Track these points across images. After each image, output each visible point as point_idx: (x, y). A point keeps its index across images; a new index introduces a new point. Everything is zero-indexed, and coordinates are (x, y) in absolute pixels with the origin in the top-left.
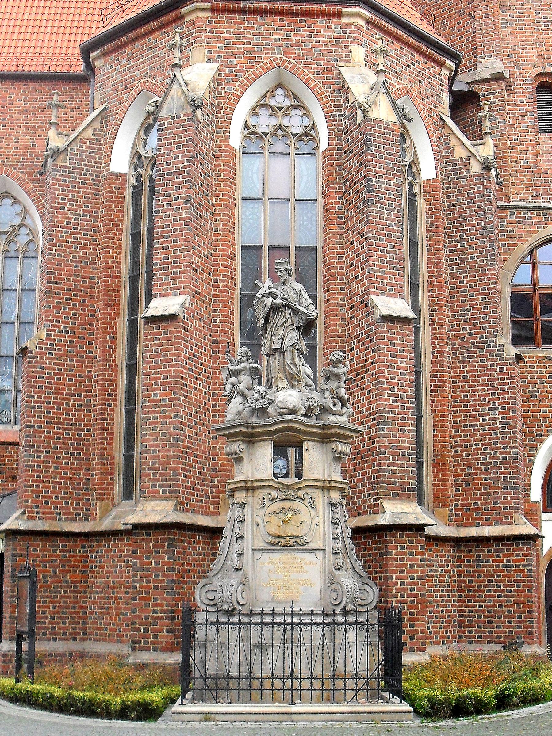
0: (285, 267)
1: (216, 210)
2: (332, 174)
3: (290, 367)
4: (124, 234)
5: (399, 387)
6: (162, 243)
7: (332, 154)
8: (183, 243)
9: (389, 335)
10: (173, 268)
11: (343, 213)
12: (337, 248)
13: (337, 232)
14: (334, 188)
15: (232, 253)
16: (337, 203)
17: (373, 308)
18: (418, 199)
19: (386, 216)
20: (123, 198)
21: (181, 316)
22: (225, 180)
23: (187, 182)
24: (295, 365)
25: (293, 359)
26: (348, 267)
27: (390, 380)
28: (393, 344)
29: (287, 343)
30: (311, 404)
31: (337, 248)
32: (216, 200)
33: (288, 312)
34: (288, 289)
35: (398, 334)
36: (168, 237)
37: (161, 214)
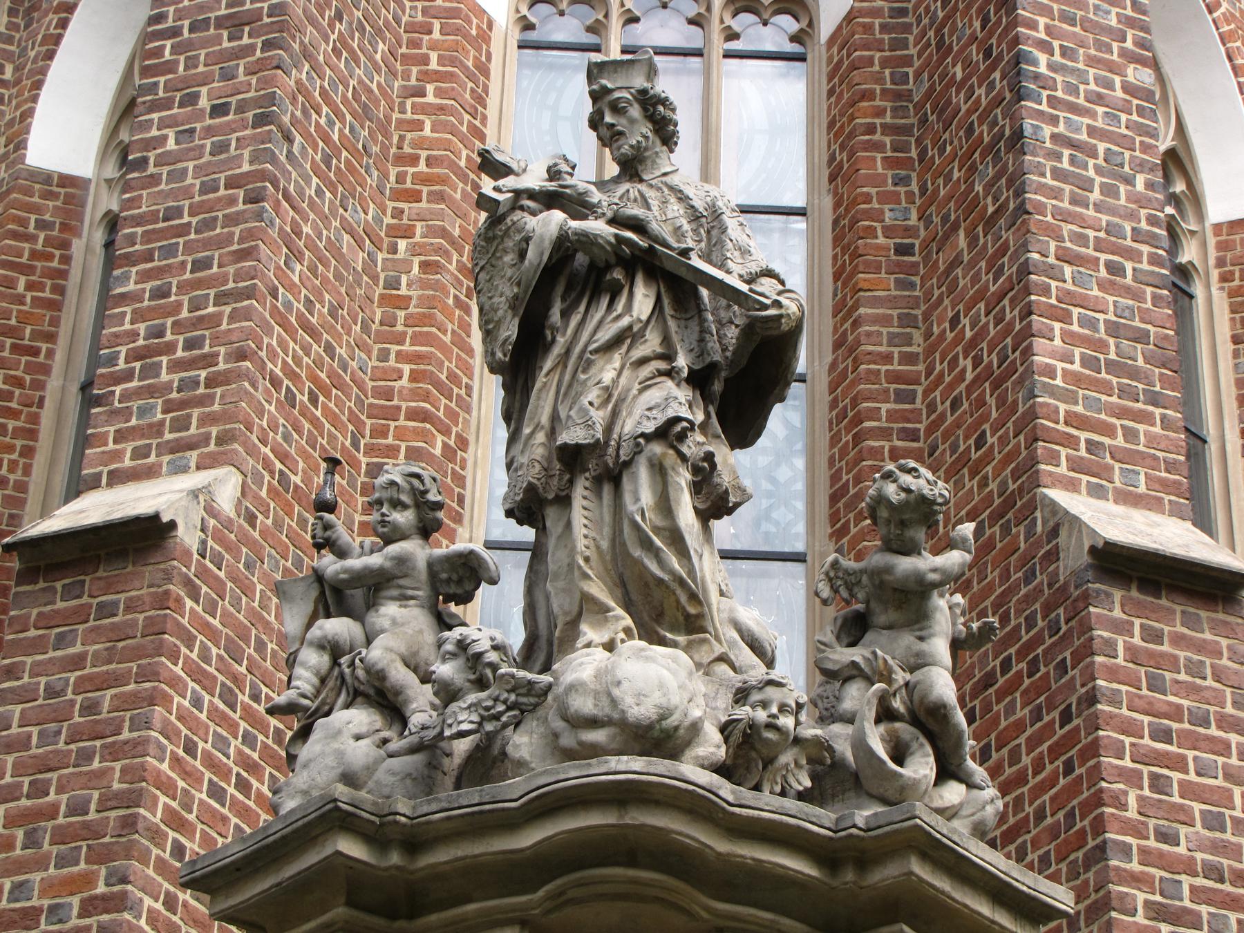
0: (639, 82)
1: (398, 213)
2: (867, 95)
3: (647, 544)
4: (54, 383)
5: (1200, 881)
6: (144, 277)
7: (868, 28)
8: (231, 270)
9: (1137, 640)
10: (175, 366)
11: (910, 231)
12: (887, 358)
13: (891, 302)
14: (879, 147)
15: (452, 377)
16: (884, 198)
17: (1054, 532)
18: (1198, 289)
19: (1095, 195)
20: (66, 259)
21: (188, 536)
22: (441, 108)
23: (267, 45)
24: (676, 539)
25: (665, 505)
26: (931, 430)
27: (1152, 843)
28: (1156, 685)
29: (638, 419)
30: (761, 715)
31: (887, 358)
32: (401, 178)
33: (642, 300)
34: (650, 194)
35: (1177, 640)
36: (170, 251)
37: (151, 169)
